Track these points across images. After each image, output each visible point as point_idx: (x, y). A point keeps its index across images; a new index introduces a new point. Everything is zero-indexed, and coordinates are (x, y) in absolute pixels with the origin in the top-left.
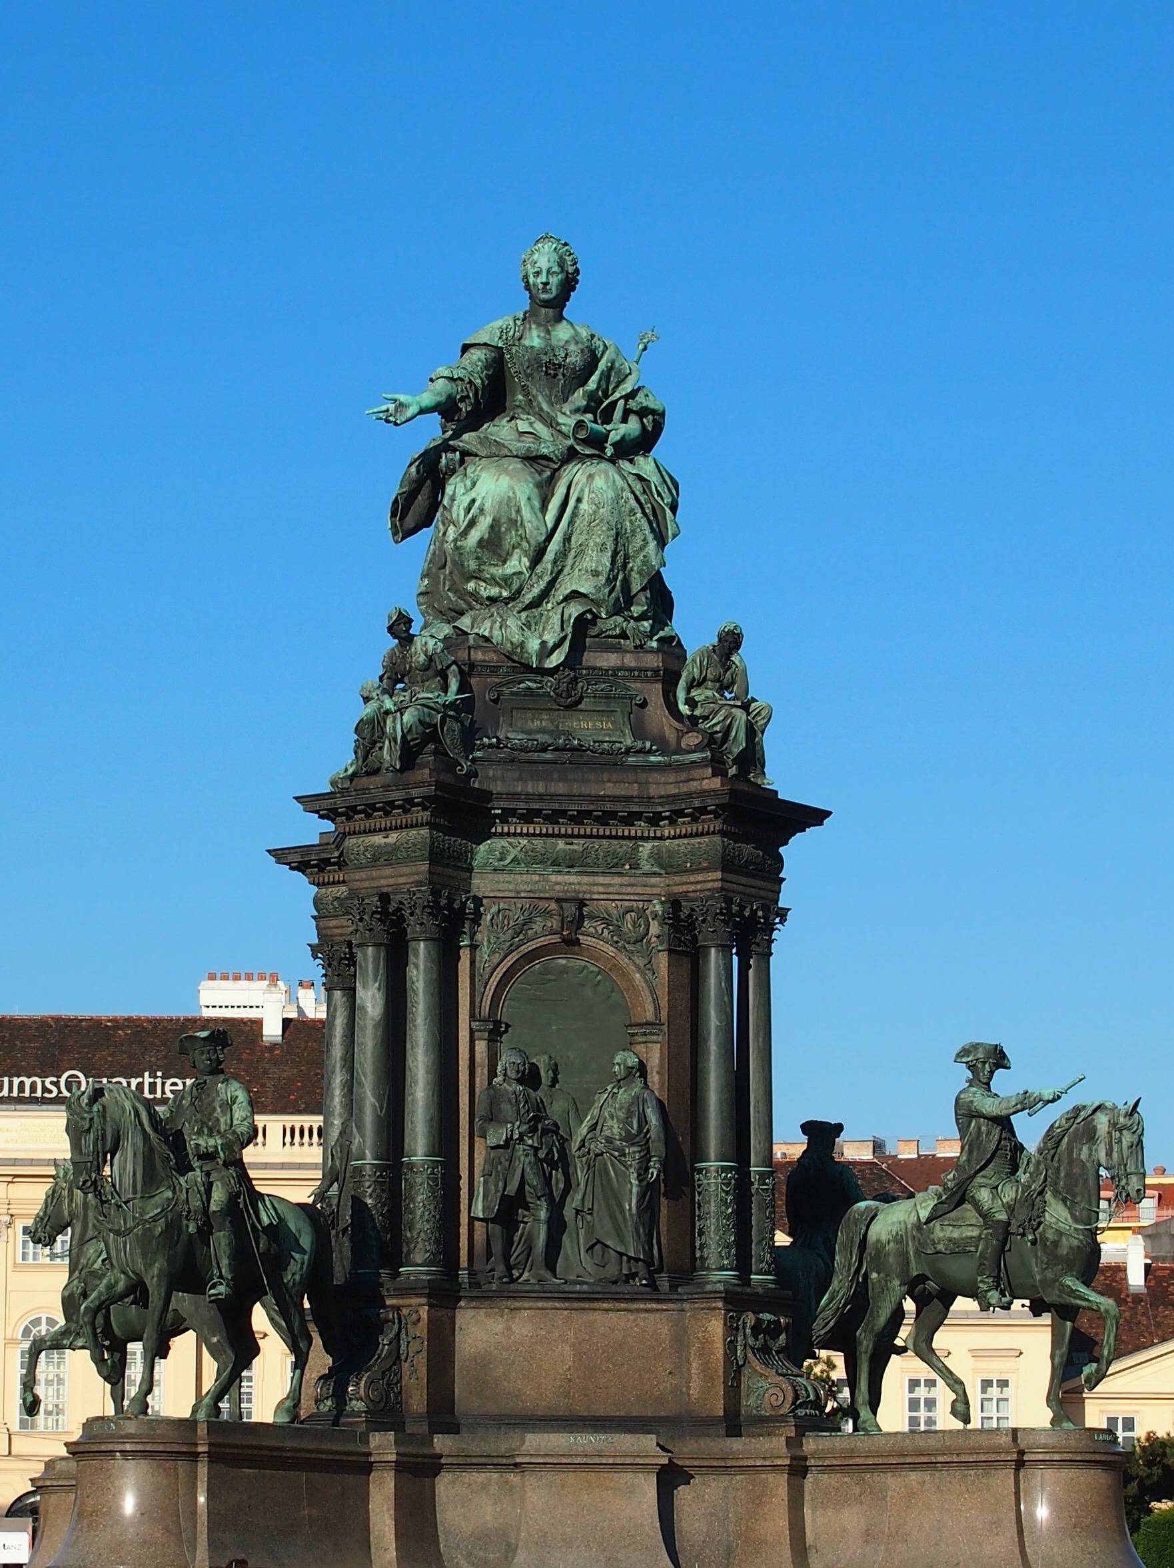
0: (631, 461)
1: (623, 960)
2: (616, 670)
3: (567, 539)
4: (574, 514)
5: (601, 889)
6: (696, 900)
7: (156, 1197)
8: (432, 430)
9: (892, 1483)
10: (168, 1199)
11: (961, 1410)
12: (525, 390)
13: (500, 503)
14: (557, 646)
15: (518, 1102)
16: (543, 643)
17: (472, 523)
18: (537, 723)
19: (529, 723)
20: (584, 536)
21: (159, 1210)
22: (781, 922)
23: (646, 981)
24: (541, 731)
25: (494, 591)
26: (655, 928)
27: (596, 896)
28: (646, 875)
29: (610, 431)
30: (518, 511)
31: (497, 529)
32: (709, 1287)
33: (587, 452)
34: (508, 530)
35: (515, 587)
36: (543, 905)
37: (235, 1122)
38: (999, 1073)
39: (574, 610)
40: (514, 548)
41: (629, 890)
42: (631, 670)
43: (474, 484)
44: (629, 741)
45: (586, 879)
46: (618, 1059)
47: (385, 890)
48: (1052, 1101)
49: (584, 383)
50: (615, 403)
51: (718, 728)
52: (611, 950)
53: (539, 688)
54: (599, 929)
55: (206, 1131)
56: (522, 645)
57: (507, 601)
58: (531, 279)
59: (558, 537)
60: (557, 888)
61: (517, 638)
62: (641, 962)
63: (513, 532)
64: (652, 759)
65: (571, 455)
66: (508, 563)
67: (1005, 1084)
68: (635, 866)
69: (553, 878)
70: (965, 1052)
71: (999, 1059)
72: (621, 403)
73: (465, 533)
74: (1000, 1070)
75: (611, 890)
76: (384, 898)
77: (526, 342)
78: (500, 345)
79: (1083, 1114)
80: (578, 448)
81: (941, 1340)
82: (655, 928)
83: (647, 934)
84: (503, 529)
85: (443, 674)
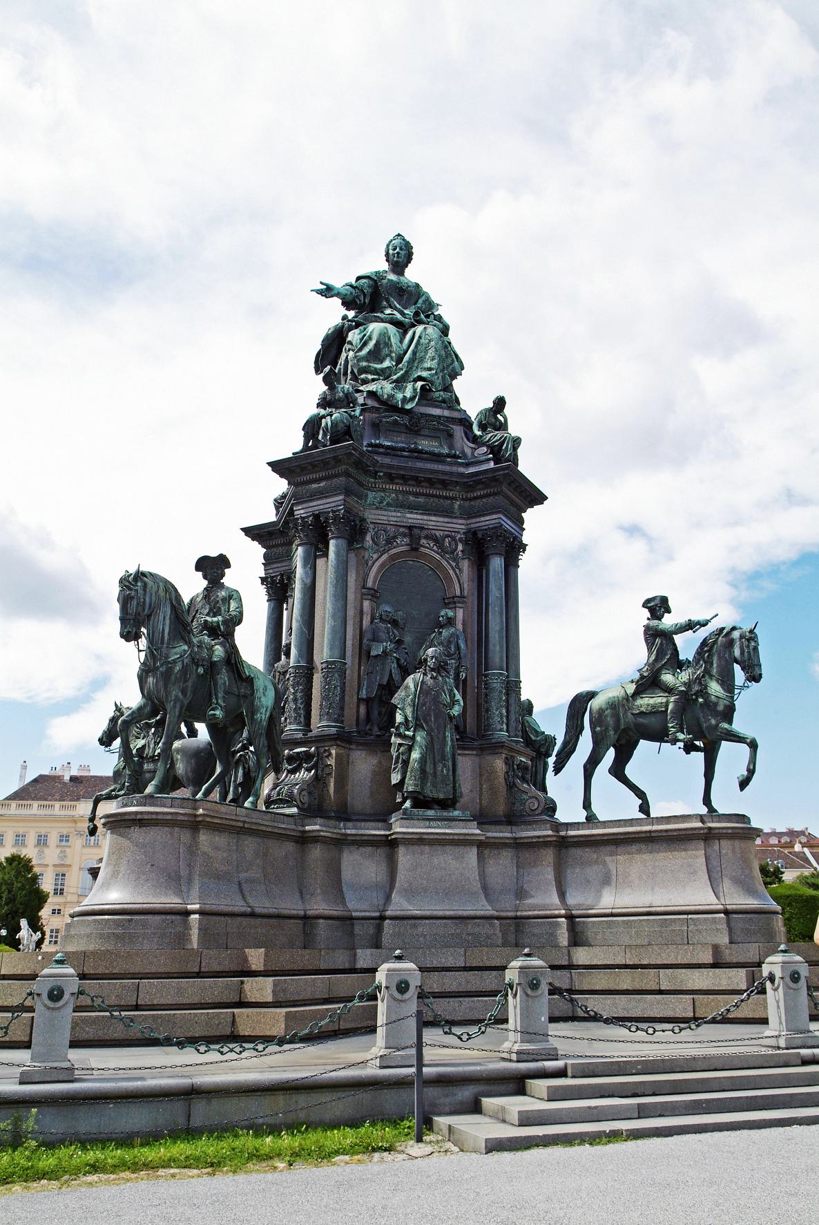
1: (445, 563)
2: (440, 417)
3: (414, 353)
5: (434, 523)
6: (486, 530)
7: (177, 649)
10: (184, 650)
11: (645, 808)
12: (388, 301)
13: (380, 334)
14: (412, 399)
15: (388, 633)
17: (365, 344)
19: (395, 438)
20: (423, 354)
21: (178, 656)
23: (456, 574)
25: (375, 377)
26: (460, 547)
27: (431, 527)
28: (455, 518)
30: (389, 339)
32: (494, 741)
34: (384, 347)
35: (387, 374)
37: (231, 610)
38: (666, 615)
39: (419, 384)
40: (387, 356)
42: (447, 417)
44: (446, 451)
45: (425, 517)
46: (442, 613)
48: (704, 625)
49: (415, 303)
52: (438, 557)
54: (432, 545)
55: (211, 614)
58: (391, 252)
60: (410, 521)
62: (454, 564)
64: (459, 460)
68: (452, 512)
69: (408, 515)
70: (648, 601)
75: (438, 524)
76: (316, 517)
79: (725, 632)
81: (630, 770)
82: (460, 547)
83: (457, 549)
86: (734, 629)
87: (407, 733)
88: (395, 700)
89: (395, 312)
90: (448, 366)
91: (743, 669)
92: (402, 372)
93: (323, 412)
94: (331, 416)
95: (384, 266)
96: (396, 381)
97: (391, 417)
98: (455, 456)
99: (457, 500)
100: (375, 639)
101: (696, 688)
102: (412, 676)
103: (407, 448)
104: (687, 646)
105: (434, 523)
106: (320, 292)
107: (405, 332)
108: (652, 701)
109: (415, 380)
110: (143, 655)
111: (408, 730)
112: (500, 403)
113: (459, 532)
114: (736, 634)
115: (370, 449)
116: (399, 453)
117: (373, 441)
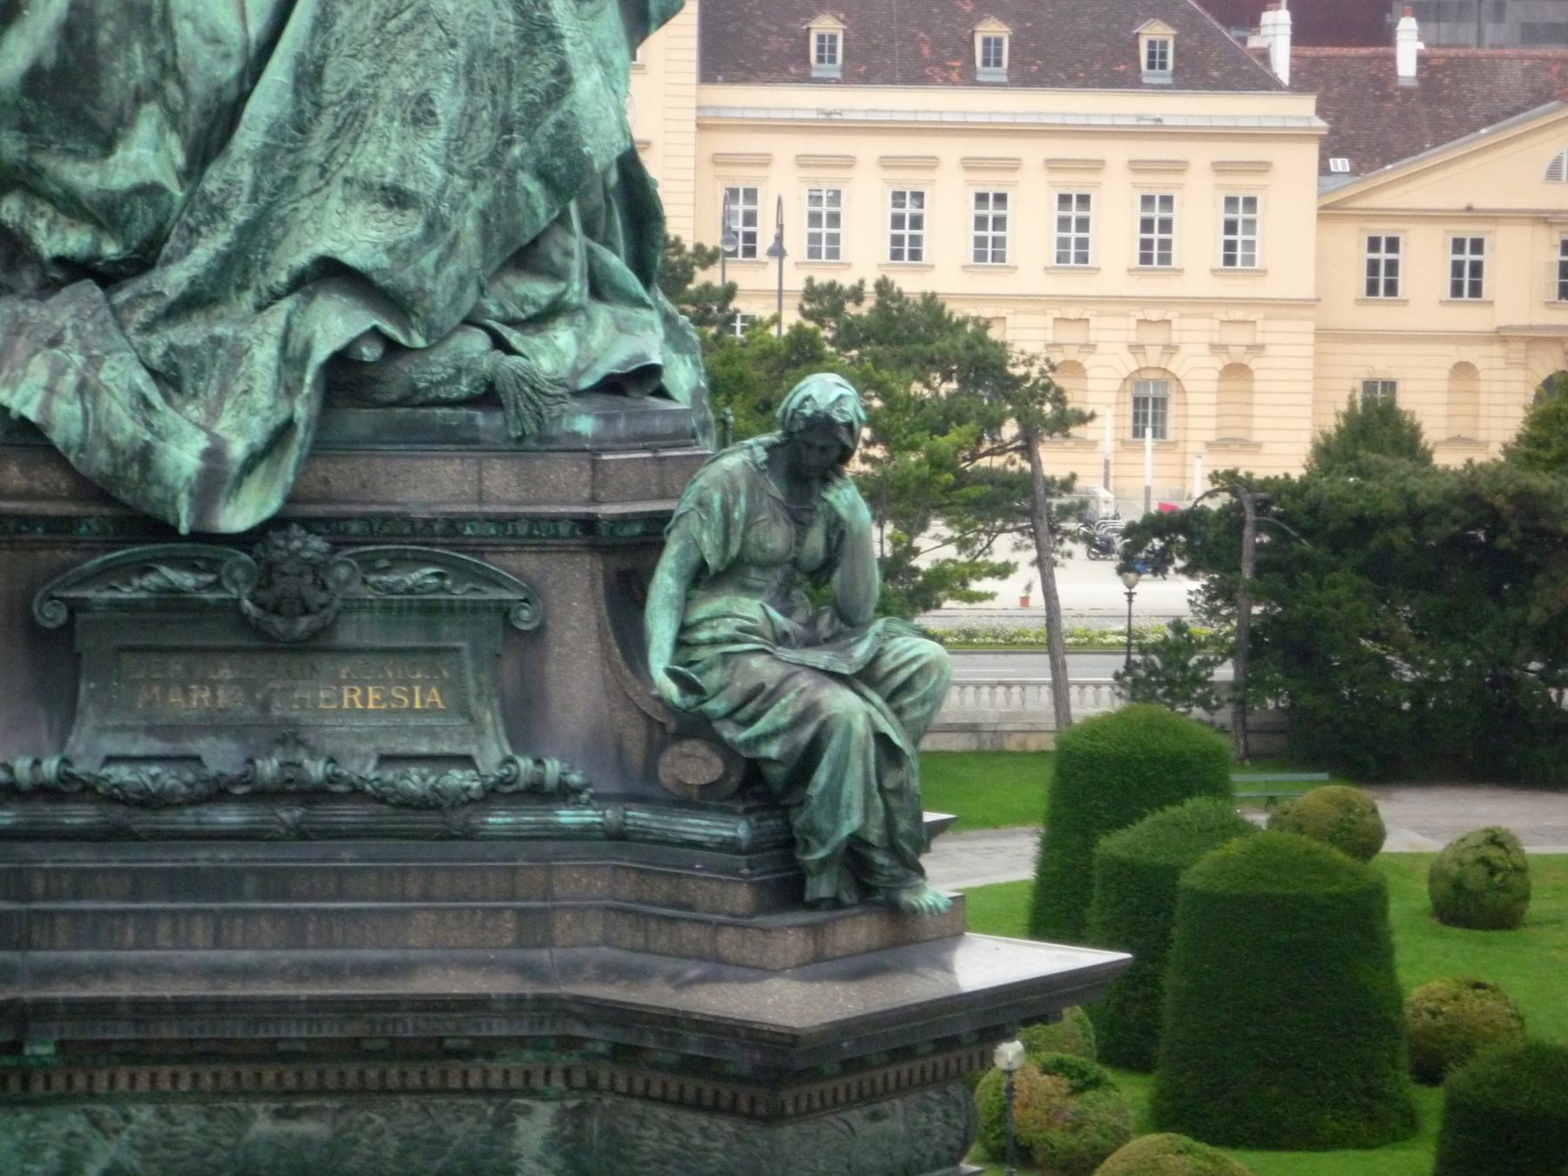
3: (308, 77)
16: (214, 455)
18: (200, 697)
19: (175, 698)
20: (362, 68)
24: (213, 725)
25: (74, 240)
31: (85, 37)
34: (121, 40)
35: (140, 229)
40: (139, 99)
42: (500, 520)
44: (492, 754)
51: (773, 750)
53: (210, 587)
56: (145, 456)
59: (278, 72)
61: (128, 428)
63: (138, 49)
64: (567, 817)
66: (120, 153)
84: (104, 38)
90: (533, 114)
97: (145, 569)
98: (540, 794)
99: (544, 1098)
103: (239, 780)
116: (187, 819)
117: (22, 766)
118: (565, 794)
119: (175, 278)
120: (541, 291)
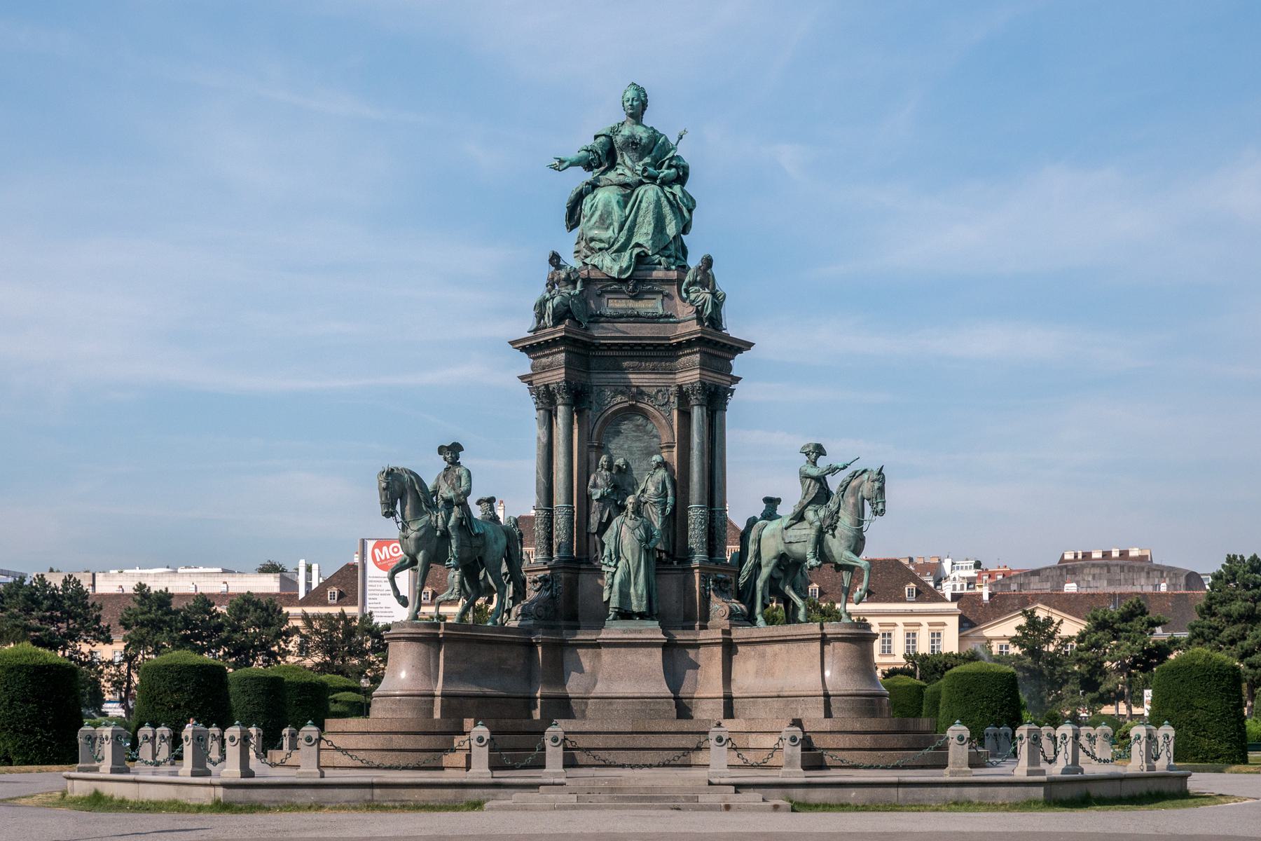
0: (670, 187)
4: (638, 208)
5: (647, 381)
8: (581, 177)
9: (770, 649)
14: (628, 268)
17: (592, 215)
22: (731, 395)
25: (602, 245)
29: (659, 173)
33: (648, 181)
36: (620, 389)
39: (637, 250)
41: (660, 381)
43: (595, 197)
44: (661, 312)
47: (546, 383)
50: (664, 162)
54: (646, 399)
57: (607, 249)
64: (671, 320)
65: (641, 183)
67: (823, 463)
71: (819, 450)
72: (667, 162)
73: (589, 221)
74: (821, 456)
76: (547, 386)
77: (622, 133)
78: (611, 135)
79: (857, 474)
80: (644, 180)
85: (574, 283)
86: (865, 471)
87: (610, 563)
88: (604, 539)
89: (627, 172)
91: (871, 504)
92: (622, 240)
93: (548, 296)
94: (553, 298)
95: (623, 117)
96: (619, 251)
100: (595, 486)
101: (828, 522)
102: (617, 518)
104: (834, 483)
105: (647, 381)
106: (555, 168)
107: (633, 191)
108: (798, 533)
109: (633, 247)
110: (400, 525)
111: (612, 561)
112: (708, 262)
113: (670, 386)
114: (865, 476)
115: (592, 320)
118: (671, 316)
119: (615, 247)
120: (669, 252)
